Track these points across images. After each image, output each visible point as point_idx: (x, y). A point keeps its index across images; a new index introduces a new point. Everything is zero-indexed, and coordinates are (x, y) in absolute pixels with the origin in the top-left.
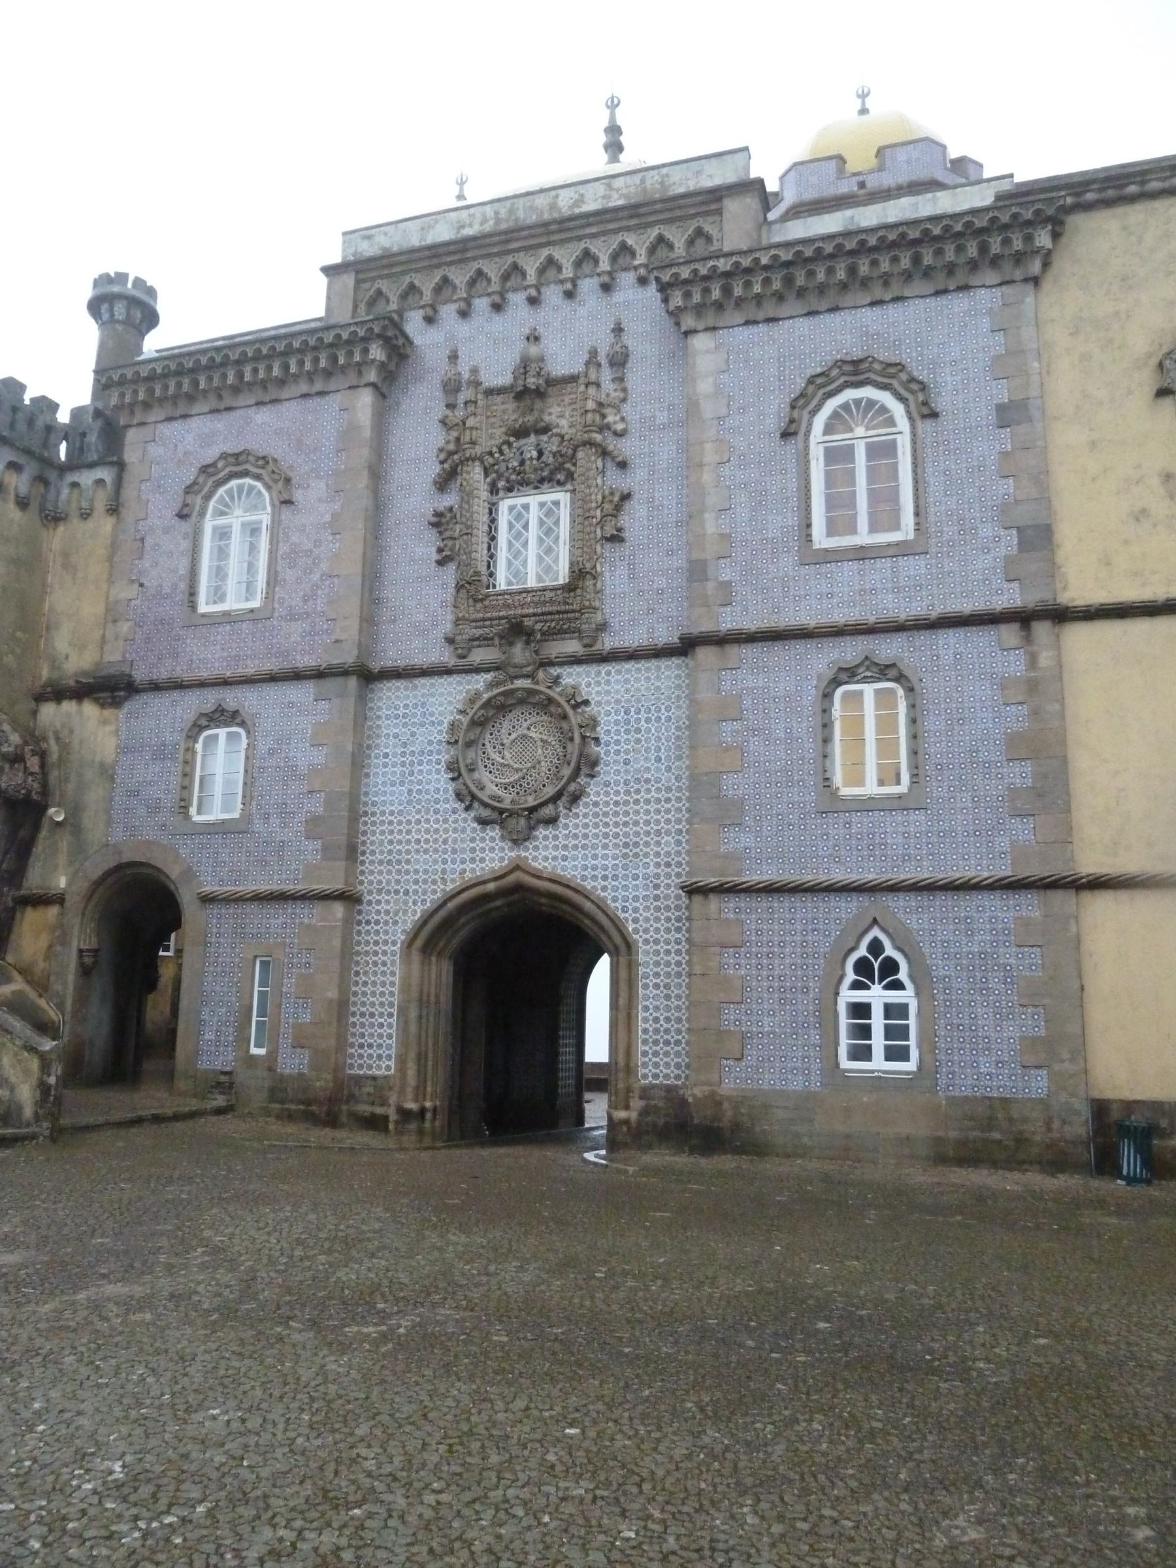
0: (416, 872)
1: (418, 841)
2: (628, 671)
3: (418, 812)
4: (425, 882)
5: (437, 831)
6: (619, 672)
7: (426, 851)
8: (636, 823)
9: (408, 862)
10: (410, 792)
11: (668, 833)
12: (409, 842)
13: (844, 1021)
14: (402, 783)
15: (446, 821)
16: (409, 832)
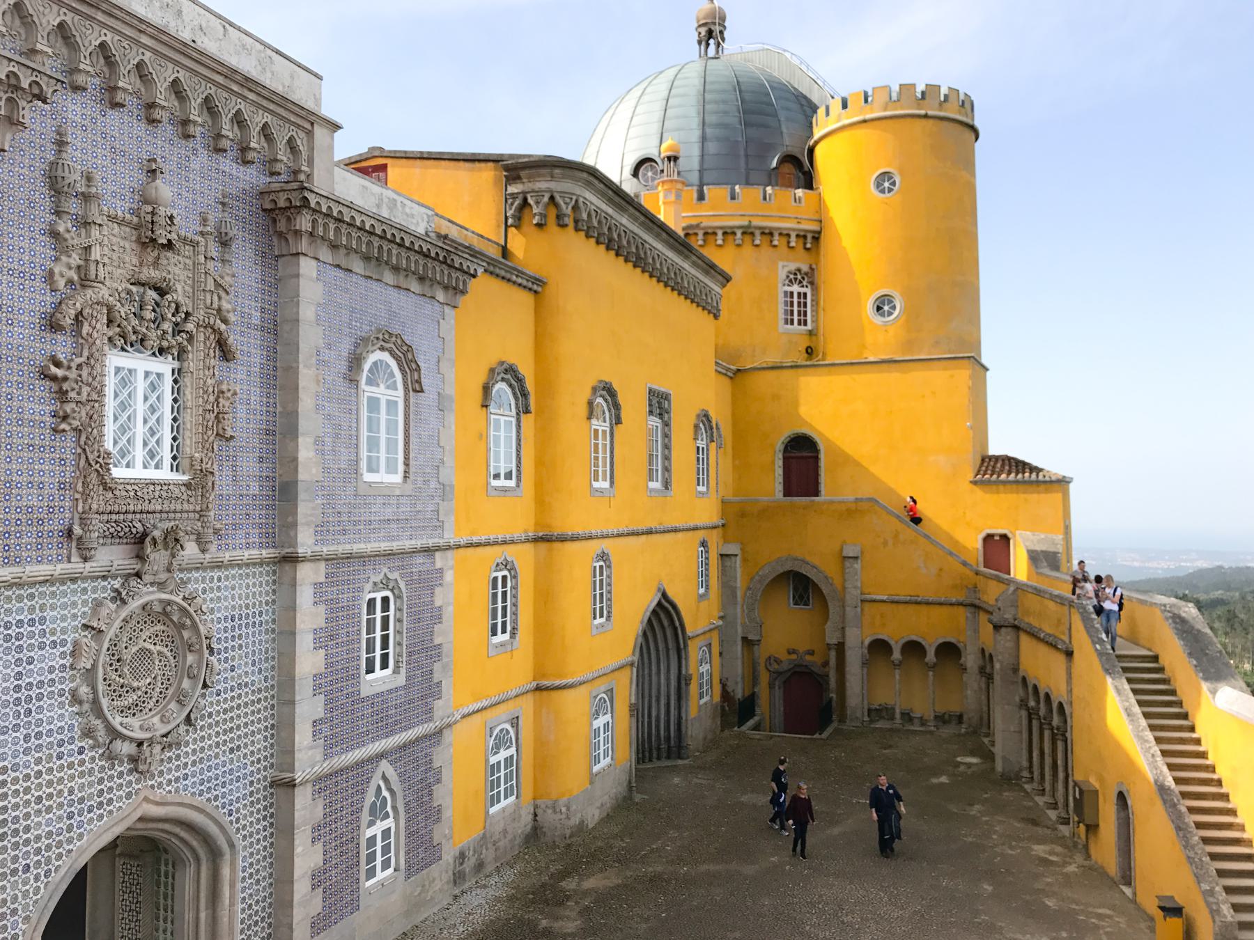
0: (38, 838)
1: (39, 799)
2: (234, 577)
3: (38, 761)
4: (49, 848)
5: (61, 780)
6: (227, 578)
7: (49, 809)
8: (238, 727)
9: (27, 829)
10: (27, 738)
11: (259, 731)
12: (28, 802)
13: (364, 853)
14: (16, 728)
15: (71, 766)
16: (27, 790)
